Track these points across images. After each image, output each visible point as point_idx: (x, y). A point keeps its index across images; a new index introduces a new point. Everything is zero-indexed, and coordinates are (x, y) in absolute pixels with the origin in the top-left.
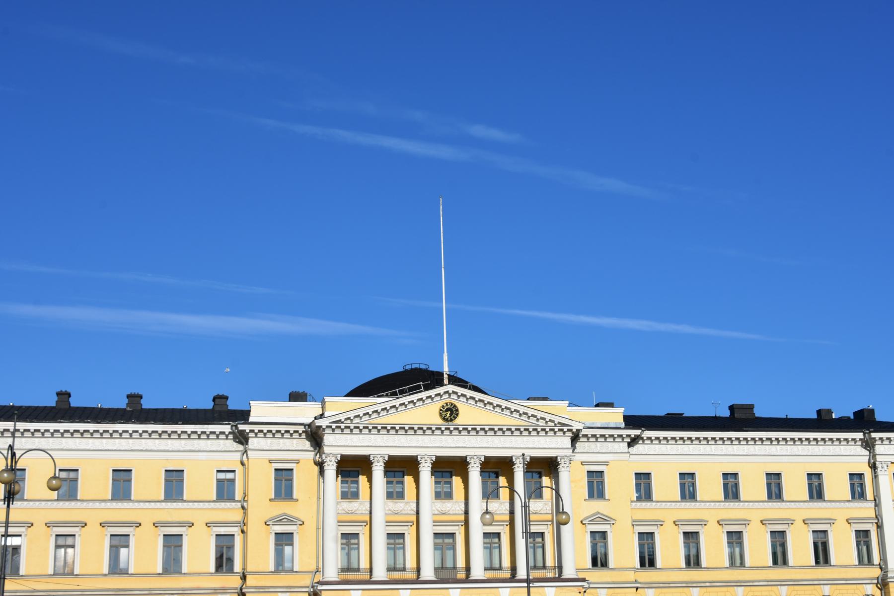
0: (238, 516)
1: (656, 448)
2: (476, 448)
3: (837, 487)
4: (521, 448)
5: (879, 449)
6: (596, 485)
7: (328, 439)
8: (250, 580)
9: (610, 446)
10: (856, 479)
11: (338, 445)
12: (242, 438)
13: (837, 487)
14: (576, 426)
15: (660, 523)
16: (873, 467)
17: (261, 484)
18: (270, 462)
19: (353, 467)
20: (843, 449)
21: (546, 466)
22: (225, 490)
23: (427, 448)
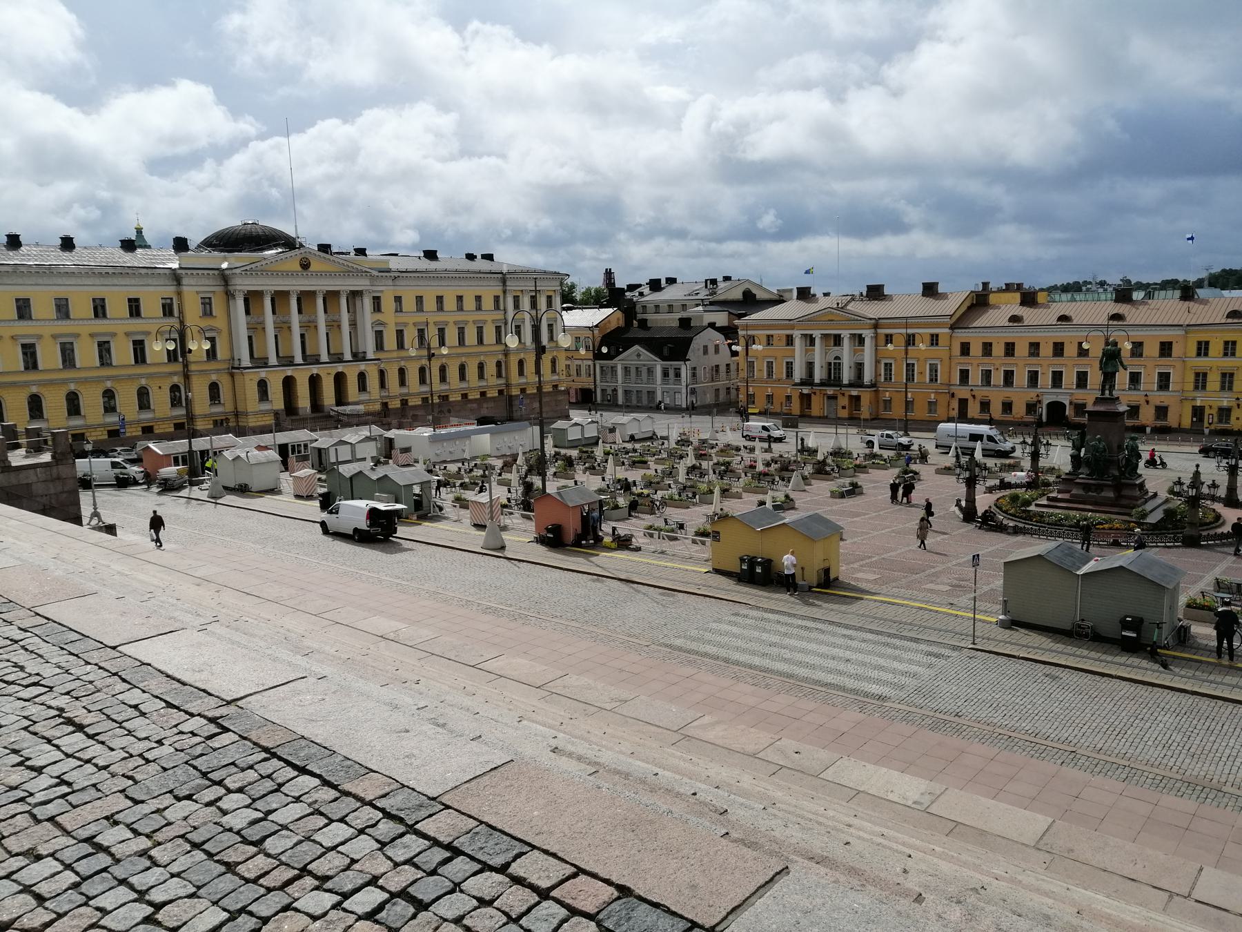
3: (488, 303)
5: (508, 283)
6: (377, 302)
8: (193, 367)
10: (497, 299)
16: (505, 292)
18: (198, 293)
22: (167, 310)
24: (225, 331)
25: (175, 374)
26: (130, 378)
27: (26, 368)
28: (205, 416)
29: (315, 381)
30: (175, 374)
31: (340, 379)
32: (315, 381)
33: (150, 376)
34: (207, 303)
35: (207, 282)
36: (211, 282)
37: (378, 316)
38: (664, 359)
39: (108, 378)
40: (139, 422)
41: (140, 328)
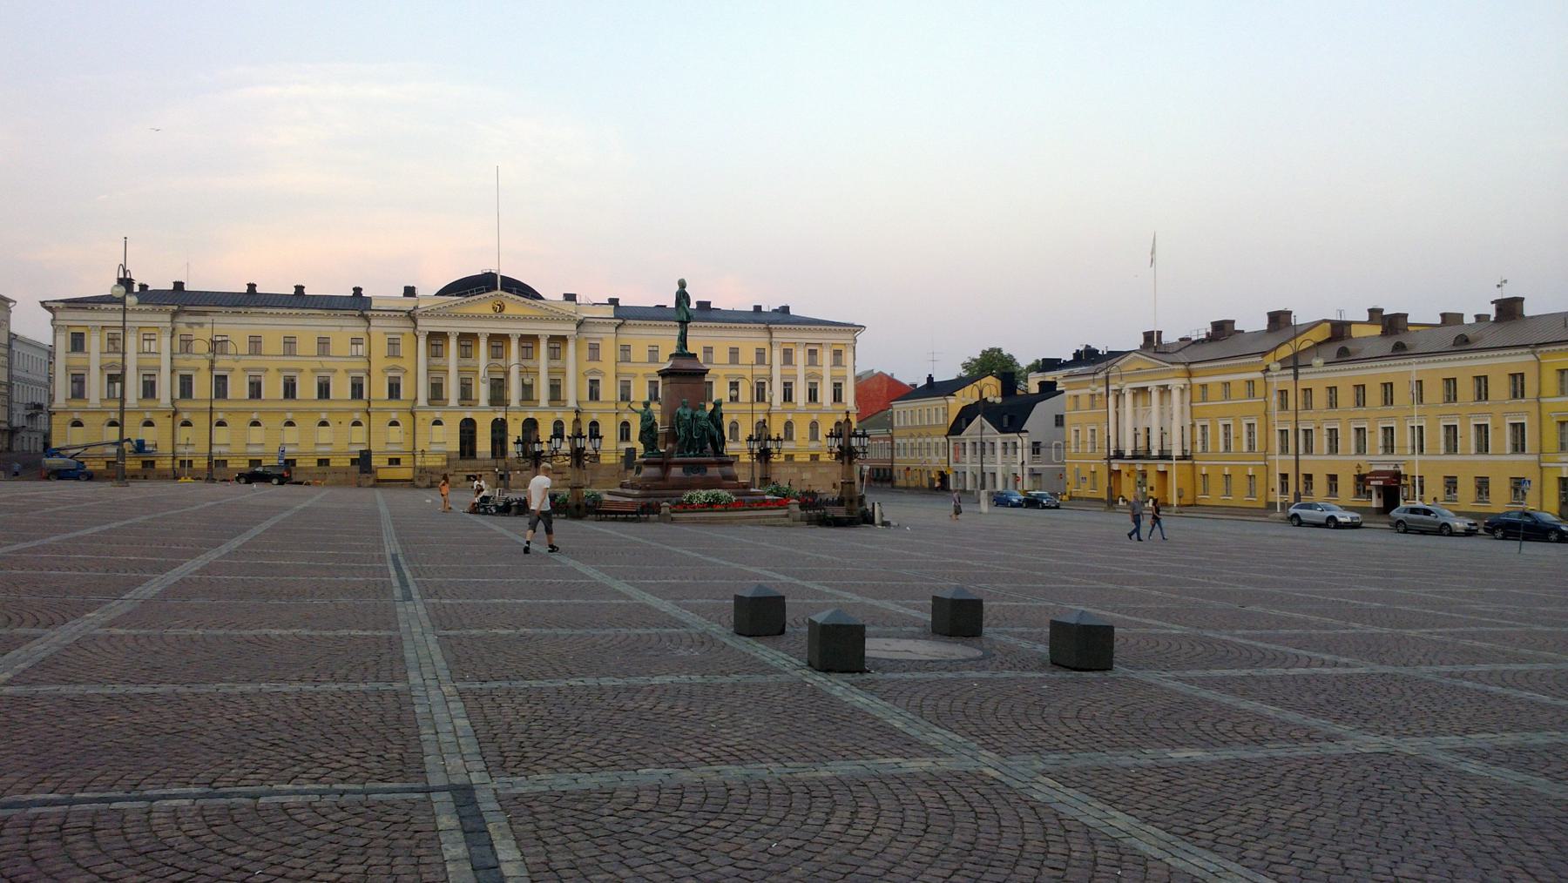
0: (365, 366)
1: (636, 331)
2: (515, 329)
4: (544, 330)
7: (420, 322)
9: (604, 329)
10: (760, 354)
11: (427, 325)
12: (367, 319)
13: (747, 355)
14: (579, 317)
15: (635, 376)
17: (380, 347)
19: (437, 339)
20: (753, 334)
21: (558, 341)
23: (484, 328)
24: (412, 371)
25: (356, 410)
26: (311, 412)
27: (252, 397)
28: (380, 453)
29: (499, 428)
30: (356, 410)
31: (531, 425)
32: (499, 428)
33: (330, 411)
34: (393, 344)
35: (396, 323)
36: (401, 323)
37: (594, 365)
38: (1003, 430)
39: (289, 410)
40: (315, 454)
41: (294, 366)
